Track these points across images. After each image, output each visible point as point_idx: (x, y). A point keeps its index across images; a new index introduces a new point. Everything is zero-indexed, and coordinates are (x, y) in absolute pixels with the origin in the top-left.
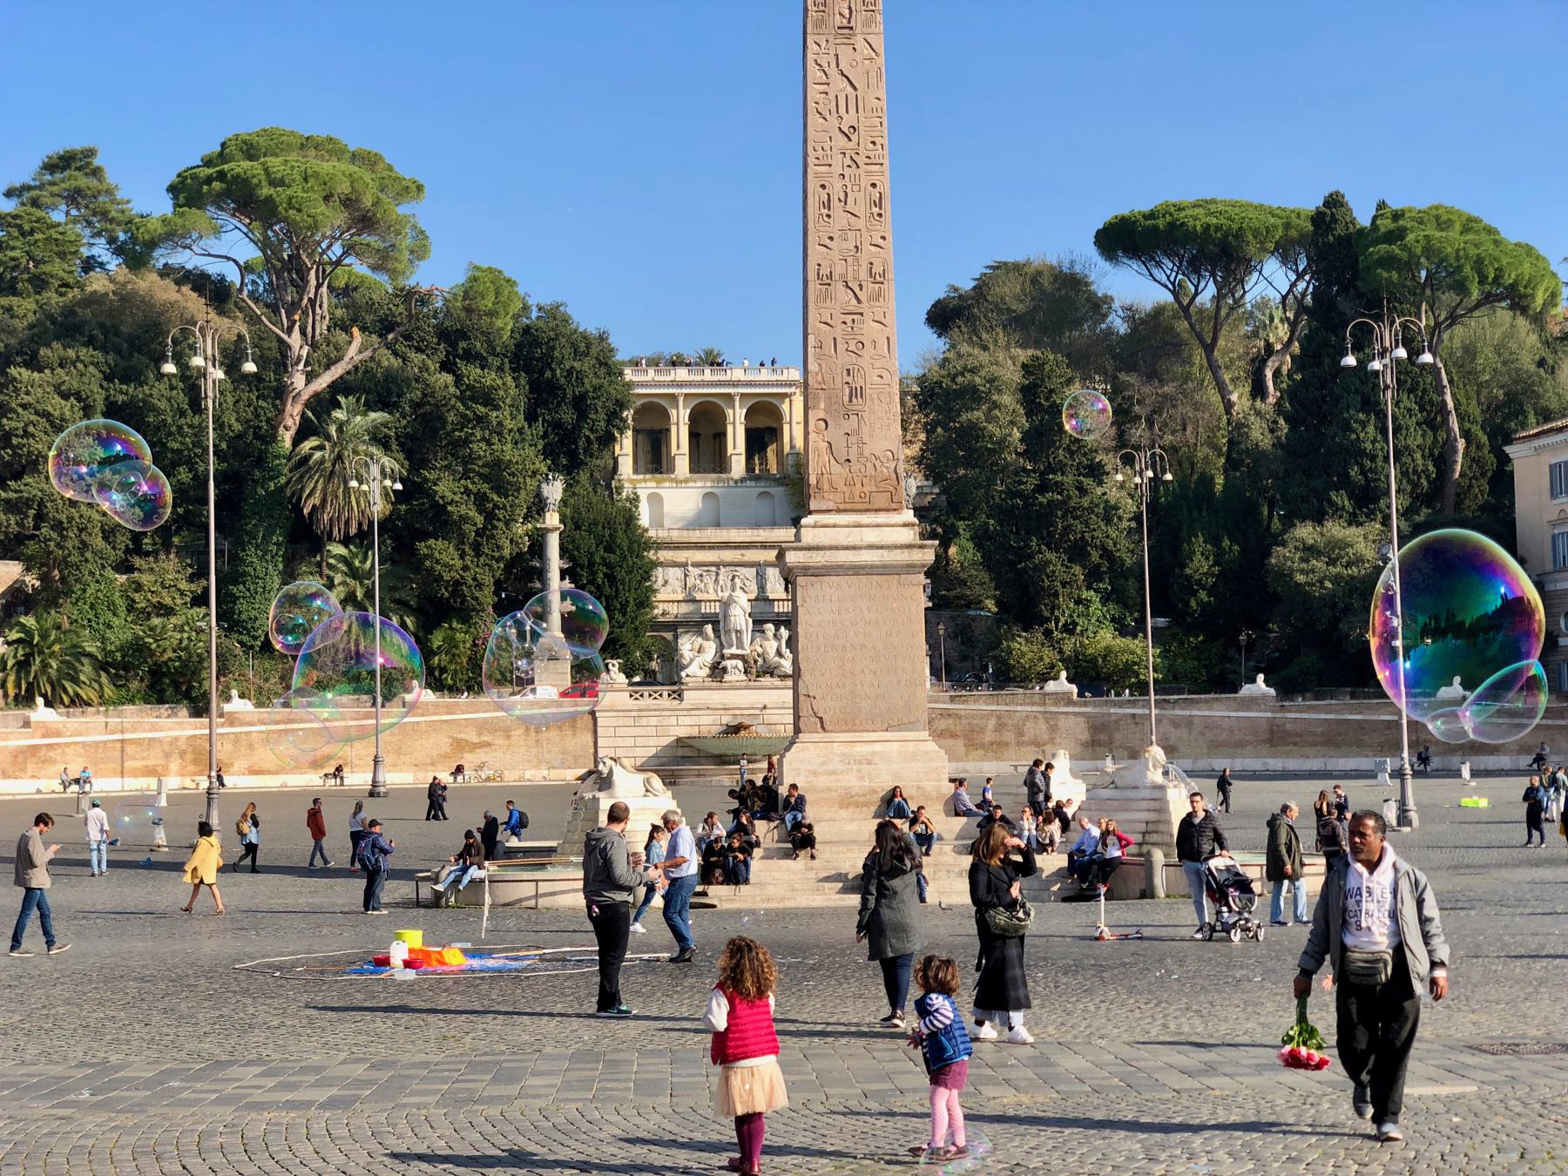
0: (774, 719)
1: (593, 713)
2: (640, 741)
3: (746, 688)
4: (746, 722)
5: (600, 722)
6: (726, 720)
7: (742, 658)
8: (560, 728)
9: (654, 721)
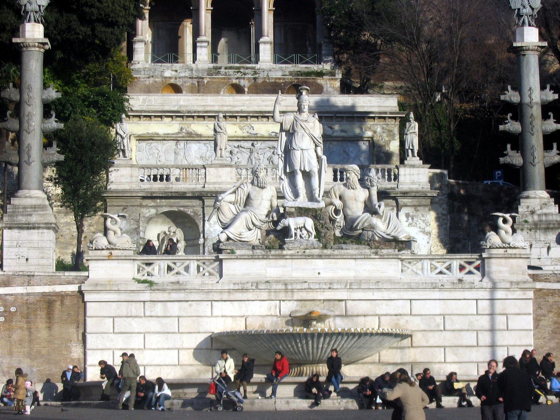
0: (363, 307)
1: (81, 293)
3: (320, 257)
4: (319, 310)
5: (91, 309)
6: (288, 307)
7: (315, 214)
9: (174, 309)
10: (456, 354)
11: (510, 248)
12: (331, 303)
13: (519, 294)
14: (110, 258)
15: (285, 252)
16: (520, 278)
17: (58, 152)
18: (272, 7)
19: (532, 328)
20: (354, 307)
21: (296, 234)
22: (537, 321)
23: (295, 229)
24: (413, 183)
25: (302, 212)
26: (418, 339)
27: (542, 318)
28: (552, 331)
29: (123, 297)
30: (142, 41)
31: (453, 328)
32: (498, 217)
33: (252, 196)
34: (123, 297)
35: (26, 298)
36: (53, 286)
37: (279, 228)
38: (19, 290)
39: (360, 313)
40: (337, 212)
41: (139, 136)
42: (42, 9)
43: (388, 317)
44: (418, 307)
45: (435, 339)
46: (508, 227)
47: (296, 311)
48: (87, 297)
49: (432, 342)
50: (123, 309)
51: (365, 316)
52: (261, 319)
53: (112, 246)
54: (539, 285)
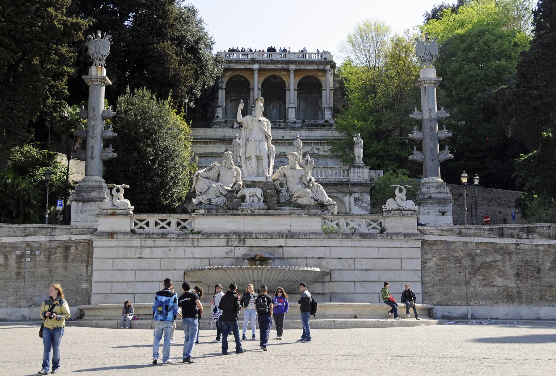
0: (295, 252)
2: (142, 276)
5: (97, 252)
6: (240, 252)
8: (49, 258)
9: (158, 252)
10: (363, 287)
11: (404, 210)
12: (272, 249)
13: (410, 243)
14: (113, 214)
15: (240, 212)
16: (411, 231)
17: (113, 151)
18: (296, 87)
19: (420, 268)
20: (288, 252)
21: (250, 200)
22: (423, 263)
23: (250, 197)
24: (360, 178)
25: (253, 184)
26: (336, 276)
27: (428, 261)
28: (436, 271)
29: (121, 244)
30: (220, 107)
31: (361, 268)
32: (396, 188)
33: (221, 174)
34: (121, 244)
35: (48, 244)
36: (70, 236)
37: (238, 195)
38: (43, 238)
39: (293, 256)
40: (282, 185)
41: (201, 154)
42: (105, 58)
43: (313, 260)
44: (336, 253)
45: (348, 276)
46: (403, 195)
47: (247, 255)
48: (95, 244)
49: (346, 278)
50: (121, 253)
51: (297, 258)
52: (221, 260)
53: (115, 207)
54: (426, 237)
